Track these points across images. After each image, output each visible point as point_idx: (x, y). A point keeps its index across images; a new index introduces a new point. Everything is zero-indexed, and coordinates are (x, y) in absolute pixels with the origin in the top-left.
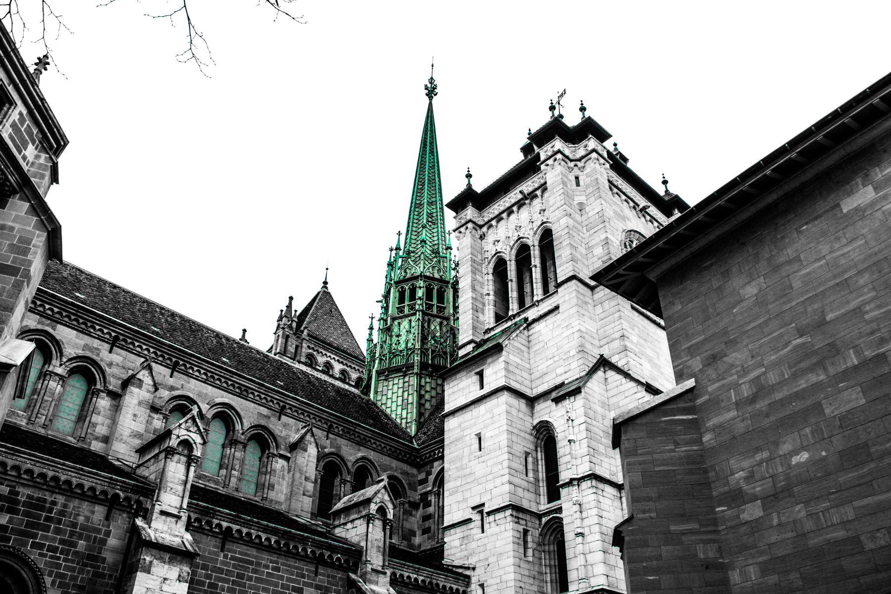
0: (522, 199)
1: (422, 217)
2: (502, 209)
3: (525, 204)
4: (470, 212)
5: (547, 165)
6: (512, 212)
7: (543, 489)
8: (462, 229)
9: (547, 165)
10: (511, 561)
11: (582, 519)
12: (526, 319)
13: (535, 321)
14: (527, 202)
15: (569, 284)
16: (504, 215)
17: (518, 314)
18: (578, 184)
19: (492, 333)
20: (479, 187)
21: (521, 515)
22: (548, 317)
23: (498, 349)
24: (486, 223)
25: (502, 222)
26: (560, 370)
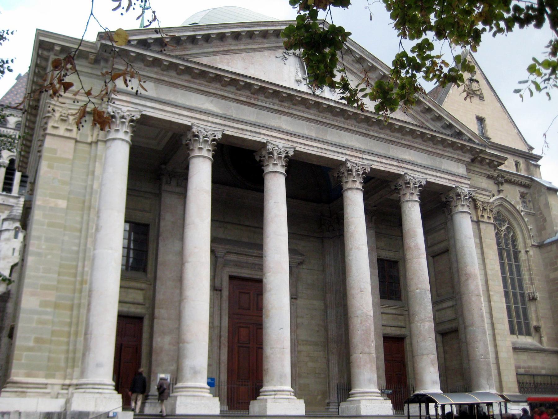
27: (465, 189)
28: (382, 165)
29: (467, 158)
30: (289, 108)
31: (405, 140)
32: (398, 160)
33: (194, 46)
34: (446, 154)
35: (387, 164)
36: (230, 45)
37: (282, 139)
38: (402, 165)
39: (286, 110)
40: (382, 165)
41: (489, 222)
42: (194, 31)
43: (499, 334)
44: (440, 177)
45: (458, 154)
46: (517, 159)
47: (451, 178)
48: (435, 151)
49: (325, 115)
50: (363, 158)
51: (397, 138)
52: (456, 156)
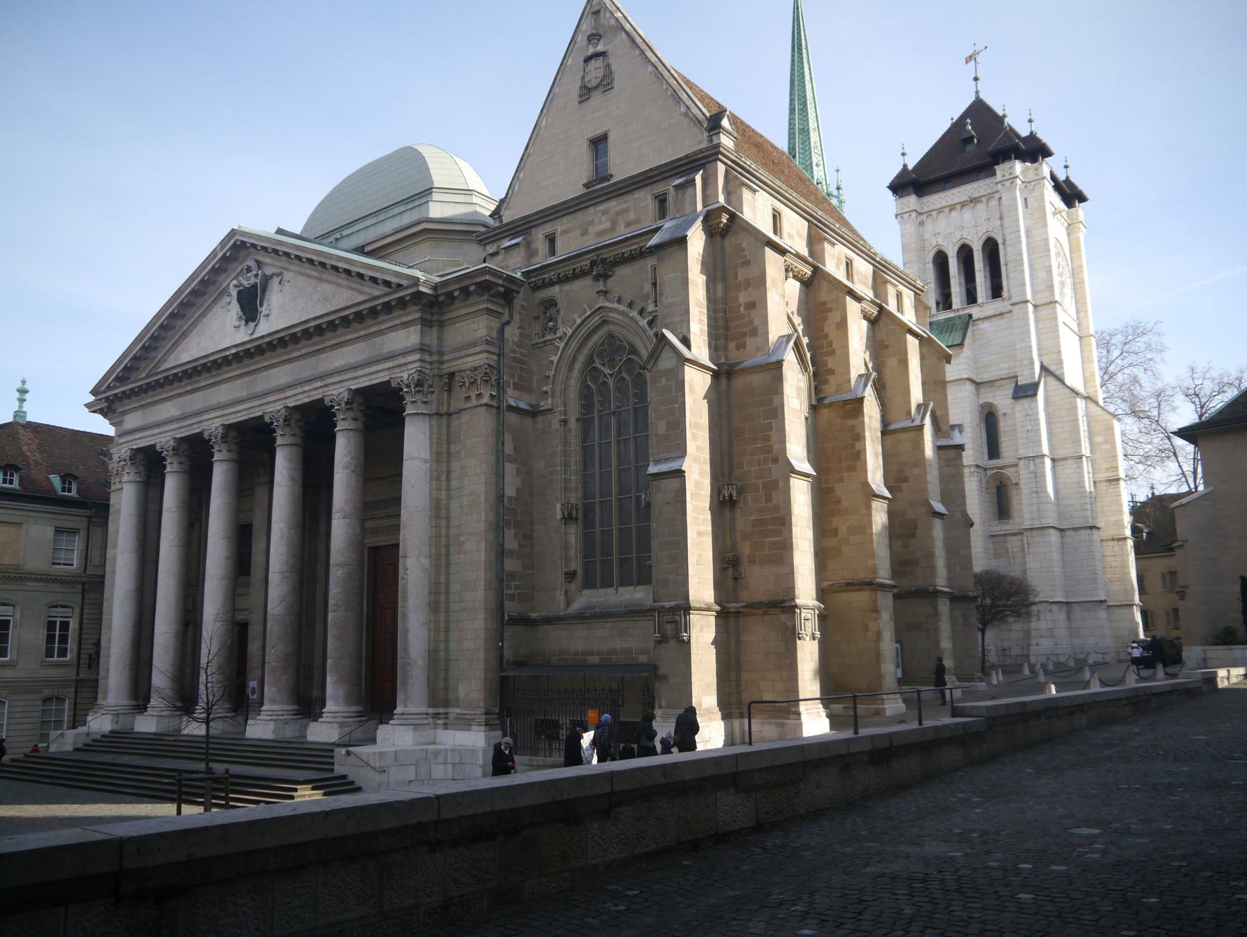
1: (807, 148)
2: (944, 204)
4: (912, 201)
5: (1003, 185)
7: (985, 451)
8: (906, 216)
9: (1003, 185)
10: (977, 501)
11: (1036, 482)
12: (970, 316)
13: (979, 319)
14: (972, 205)
15: (1023, 305)
17: (963, 309)
18: (1027, 207)
19: (935, 319)
20: (910, 167)
21: (979, 470)
22: (993, 319)
23: (961, 345)
24: (926, 212)
25: (942, 216)
26: (1002, 366)
27: (405, 375)
29: (414, 313)
30: (219, 375)
31: (328, 340)
32: (321, 378)
34: (383, 327)
35: (311, 390)
36: (182, 326)
37: (218, 417)
39: (218, 379)
40: (306, 395)
41: (479, 403)
43: (465, 609)
44: (376, 372)
46: (659, 188)
47: (391, 364)
48: (367, 332)
50: (286, 398)
51: (318, 343)
52: (398, 322)
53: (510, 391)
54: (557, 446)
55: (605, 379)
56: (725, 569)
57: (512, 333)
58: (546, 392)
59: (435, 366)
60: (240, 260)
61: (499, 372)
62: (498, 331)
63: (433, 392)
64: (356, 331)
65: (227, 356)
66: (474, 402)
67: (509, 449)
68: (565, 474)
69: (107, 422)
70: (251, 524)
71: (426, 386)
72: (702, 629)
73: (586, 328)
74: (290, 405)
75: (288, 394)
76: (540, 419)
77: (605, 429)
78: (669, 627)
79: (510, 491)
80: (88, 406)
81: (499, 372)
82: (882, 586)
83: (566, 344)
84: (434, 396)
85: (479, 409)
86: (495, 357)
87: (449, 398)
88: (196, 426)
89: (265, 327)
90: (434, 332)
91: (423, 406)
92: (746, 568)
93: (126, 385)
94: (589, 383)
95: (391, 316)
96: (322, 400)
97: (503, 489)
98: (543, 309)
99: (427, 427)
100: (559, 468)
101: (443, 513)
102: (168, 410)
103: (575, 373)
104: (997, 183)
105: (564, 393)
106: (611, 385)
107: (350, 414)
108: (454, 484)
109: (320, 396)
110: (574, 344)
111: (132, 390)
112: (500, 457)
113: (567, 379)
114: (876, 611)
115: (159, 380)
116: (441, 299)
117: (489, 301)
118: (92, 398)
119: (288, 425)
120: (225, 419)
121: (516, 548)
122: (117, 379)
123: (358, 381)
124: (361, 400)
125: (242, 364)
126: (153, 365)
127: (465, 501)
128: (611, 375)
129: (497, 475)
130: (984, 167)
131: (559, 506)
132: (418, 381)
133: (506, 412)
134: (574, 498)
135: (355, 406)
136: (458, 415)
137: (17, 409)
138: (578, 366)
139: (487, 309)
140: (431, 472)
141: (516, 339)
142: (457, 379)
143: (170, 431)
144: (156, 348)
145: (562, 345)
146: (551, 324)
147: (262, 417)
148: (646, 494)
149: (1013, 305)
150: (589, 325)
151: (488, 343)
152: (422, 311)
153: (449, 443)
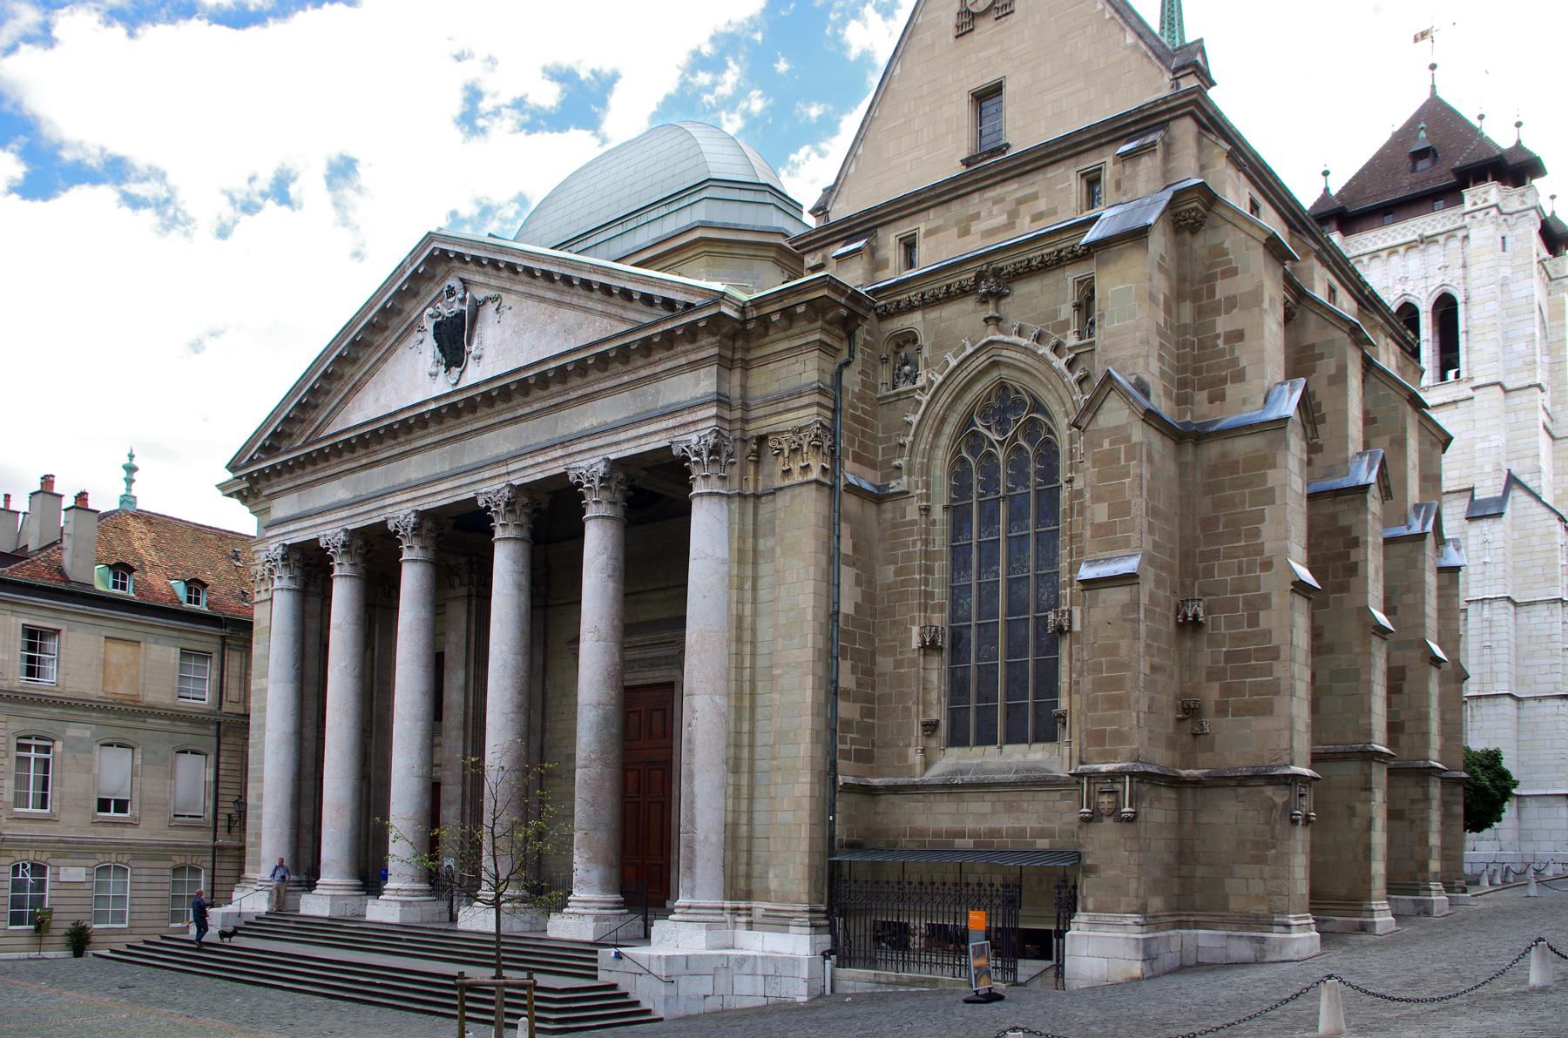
0: (1416, 241)
2: (1381, 246)
3: (1416, 247)
6: (1396, 252)
14: (1422, 247)
16: (1384, 254)
20: (1334, 191)
27: (694, 436)
28: (540, 469)
29: (708, 348)
30: (408, 442)
31: (573, 389)
32: (562, 444)
33: (317, 410)
35: (546, 462)
36: (352, 375)
37: (408, 501)
38: (570, 450)
39: (407, 448)
41: (805, 479)
42: (296, 396)
44: (646, 435)
45: (684, 352)
47: (671, 423)
48: (634, 377)
49: (448, 424)
50: (508, 473)
51: (558, 394)
52: (683, 361)
53: (849, 464)
54: (914, 543)
55: (992, 450)
56: (1179, 720)
57: (852, 379)
58: (899, 468)
59: (738, 425)
60: (436, 279)
61: (834, 436)
62: (832, 375)
63: (733, 464)
64: (618, 375)
65: (422, 414)
66: (797, 478)
67: (846, 546)
68: (927, 584)
69: (246, 509)
70: (443, 653)
71: (724, 454)
72: (1151, 803)
73: (965, 373)
74: (516, 483)
75: (512, 467)
76: (888, 506)
77: (989, 519)
78: (1105, 799)
79: (847, 607)
80: (222, 487)
81: (834, 436)
82: (1380, 753)
83: (933, 397)
84: (736, 470)
85: (804, 489)
86: (829, 414)
87: (756, 473)
88: (375, 514)
89: (474, 373)
90: (736, 377)
91: (718, 483)
92: (1209, 721)
93: (276, 457)
94: (965, 454)
95: (673, 352)
96: (564, 475)
97: (838, 603)
98: (894, 348)
99: (725, 513)
100: (917, 577)
101: (747, 636)
102: (336, 491)
103: (944, 441)
104: (1464, 215)
105: (926, 470)
106: (1001, 458)
107: (605, 495)
108: (763, 595)
109: (562, 470)
110: (944, 398)
111: (285, 463)
112: (834, 558)
113: (931, 448)
114: (1370, 789)
115: (323, 448)
116: (750, 326)
117: (823, 330)
118: (230, 476)
119: (512, 511)
120: (417, 503)
121: (855, 688)
122: (263, 448)
123: (620, 447)
124: (621, 476)
125: (444, 426)
126: (312, 430)
127: (782, 619)
128: (1001, 443)
129: (829, 584)
130: (1449, 194)
131: (915, 630)
132: (715, 446)
133: (844, 495)
134: (939, 619)
135: (613, 484)
136: (770, 497)
137: (124, 492)
138: (949, 429)
139: (820, 341)
140: (730, 576)
141: (857, 390)
142: (770, 444)
143: (338, 520)
144: (315, 407)
145: (925, 399)
146: (907, 368)
147: (474, 500)
148: (1056, 613)
149: (1474, 389)
150: (969, 369)
151: (821, 391)
152: (721, 344)
153: (755, 537)
